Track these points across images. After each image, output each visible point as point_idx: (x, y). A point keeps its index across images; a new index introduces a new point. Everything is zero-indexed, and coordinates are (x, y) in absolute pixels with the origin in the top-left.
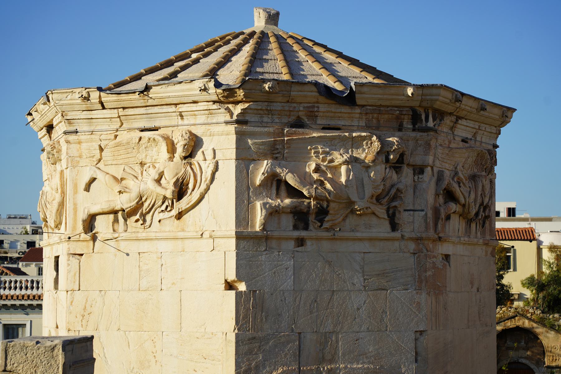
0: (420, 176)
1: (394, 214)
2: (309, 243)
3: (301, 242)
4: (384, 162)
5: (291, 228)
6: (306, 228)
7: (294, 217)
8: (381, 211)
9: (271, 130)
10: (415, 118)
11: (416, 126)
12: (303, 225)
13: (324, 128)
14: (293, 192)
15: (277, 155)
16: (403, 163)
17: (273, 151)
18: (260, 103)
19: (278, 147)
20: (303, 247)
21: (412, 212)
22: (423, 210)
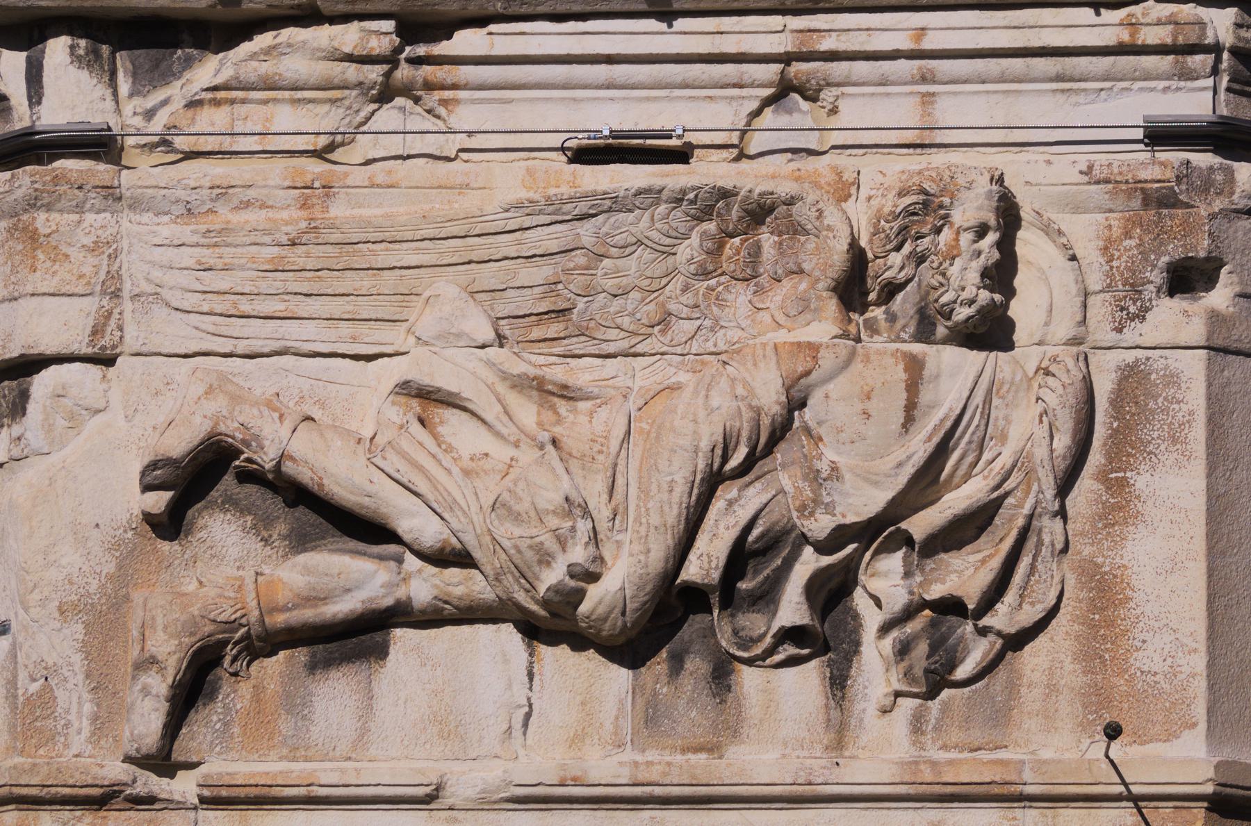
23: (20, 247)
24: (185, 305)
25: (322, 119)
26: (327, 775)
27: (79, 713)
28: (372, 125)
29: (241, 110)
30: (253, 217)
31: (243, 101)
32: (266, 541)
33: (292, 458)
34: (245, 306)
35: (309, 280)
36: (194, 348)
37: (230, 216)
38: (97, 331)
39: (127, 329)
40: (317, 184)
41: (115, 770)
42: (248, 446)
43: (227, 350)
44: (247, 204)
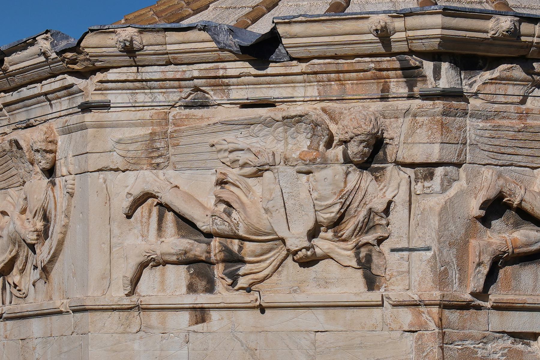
0: (427, 184)
1: (369, 258)
2: (214, 315)
3: (200, 314)
4: (342, 161)
5: (184, 289)
6: (210, 289)
7: (188, 270)
8: (345, 252)
9: (147, 114)
10: (411, 75)
11: (415, 89)
12: (204, 283)
13: (244, 106)
14: (186, 224)
15: (159, 160)
16: (384, 161)
17: (150, 153)
18: (124, 69)
19: (158, 145)
20: (205, 324)
21: (406, 253)
22: (428, 249)
23: (436, 127)
24: (485, 149)
25: (519, 90)
26: (530, 300)
27: (455, 277)
28: (534, 94)
29: (498, 86)
30: (506, 122)
31: (499, 83)
32: (507, 225)
33: (525, 201)
34: (503, 150)
35: (522, 143)
36: (487, 162)
37: (498, 121)
38: (459, 156)
39: (467, 155)
40: (524, 112)
41: (468, 297)
42: (510, 195)
43: (495, 164)
44: (504, 117)
